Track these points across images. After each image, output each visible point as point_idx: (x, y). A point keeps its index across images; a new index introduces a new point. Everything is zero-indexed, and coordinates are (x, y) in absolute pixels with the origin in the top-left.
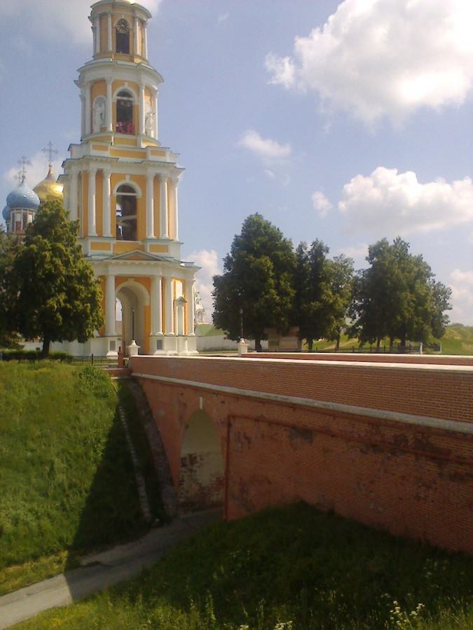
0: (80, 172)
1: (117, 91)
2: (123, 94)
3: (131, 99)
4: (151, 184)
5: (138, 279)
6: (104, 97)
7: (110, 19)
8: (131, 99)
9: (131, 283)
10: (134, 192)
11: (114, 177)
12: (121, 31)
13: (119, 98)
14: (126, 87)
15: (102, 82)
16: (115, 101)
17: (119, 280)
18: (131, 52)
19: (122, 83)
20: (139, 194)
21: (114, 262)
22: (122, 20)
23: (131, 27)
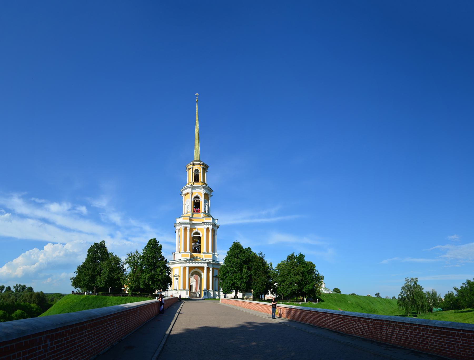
0: (179, 228)
1: (194, 196)
2: (197, 197)
3: (199, 199)
4: (205, 231)
5: (199, 268)
6: (189, 199)
8: (199, 199)
9: (197, 270)
11: (191, 230)
12: (196, 174)
13: (195, 199)
14: (196, 195)
15: (188, 193)
16: (193, 200)
17: (190, 268)
18: (199, 181)
19: (196, 193)
20: (201, 235)
21: (188, 261)
22: (196, 169)
23: (200, 172)
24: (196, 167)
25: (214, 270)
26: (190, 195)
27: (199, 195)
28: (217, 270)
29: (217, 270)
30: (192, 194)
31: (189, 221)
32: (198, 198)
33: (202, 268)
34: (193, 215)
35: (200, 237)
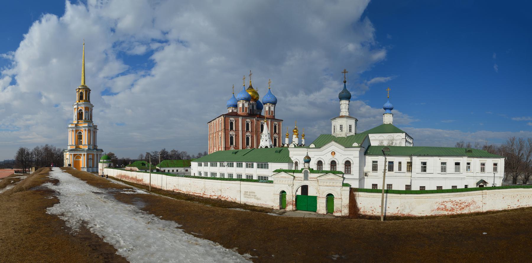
1: (79, 110)
2: (81, 110)
5: (79, 154)
7: (78, 92)
10: (82, 133)
17: (74, 155)
24: (80, 91)
25: (89, 155)
26: (76, 109)
27: (82, 109)
28: (92, 155)
29: (92, 155)
30: (78, 108)
31: (74, 126)
32: (82, 110)
33: (81, 155)
34: (78, 122)
35: (82, 135)
